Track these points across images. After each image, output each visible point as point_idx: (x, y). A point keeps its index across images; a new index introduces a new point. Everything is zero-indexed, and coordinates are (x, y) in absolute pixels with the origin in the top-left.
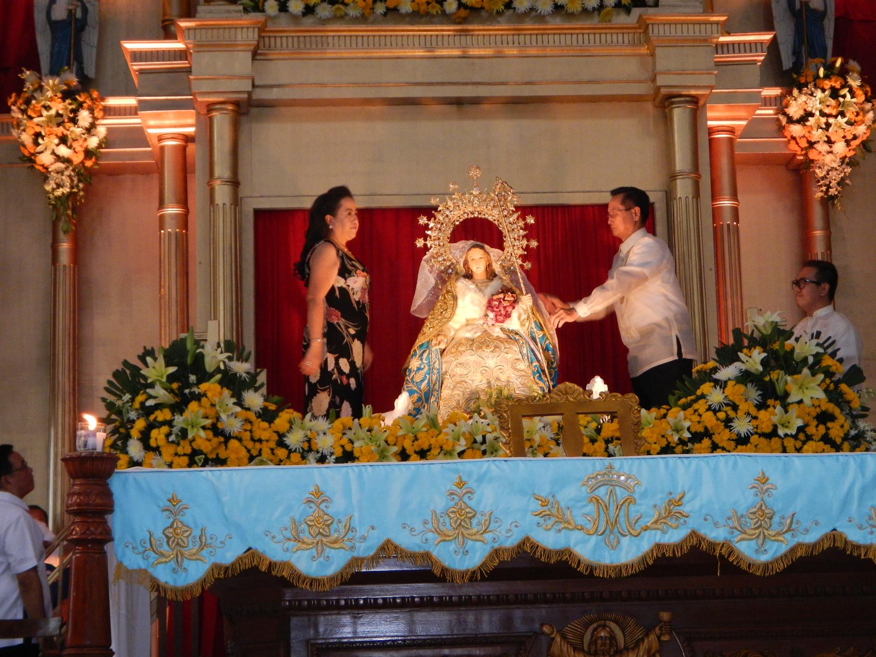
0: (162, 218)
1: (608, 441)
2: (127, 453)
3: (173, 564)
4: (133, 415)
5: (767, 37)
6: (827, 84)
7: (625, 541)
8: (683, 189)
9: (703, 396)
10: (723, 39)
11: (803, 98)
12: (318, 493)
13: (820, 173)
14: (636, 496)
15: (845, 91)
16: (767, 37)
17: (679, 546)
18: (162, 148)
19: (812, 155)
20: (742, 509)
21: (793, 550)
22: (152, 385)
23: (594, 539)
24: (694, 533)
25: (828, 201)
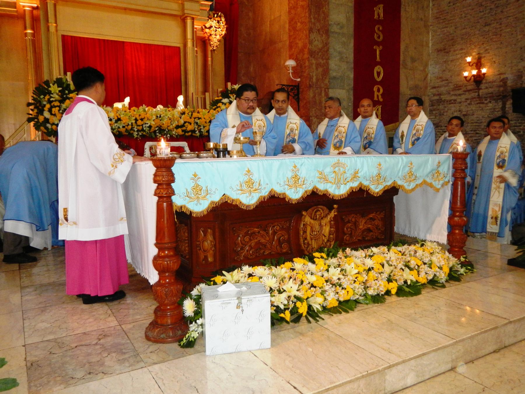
0: (26, 34)
1: (195, 118)
2: (43, 115)
3: (195, 202)
4: (45, 103)
5: (210, 3)
6: (217, 19)
7: (342, 186)
8: (190, 44)
9: (219, 107)
10: (202, 2)
11: (211, 22)
12: (249, 171)
13: (212, 43)
14: (346, 171)
15: (221, 22)
16: (210, 3)
17: (357, 187)
18: (25, 10)
19: (210, 38)
20: (374, 175)
21: (384, 187)
22: (52, 94)
23: (334, 186)
24: (361, 183)
25: (213, 51)
